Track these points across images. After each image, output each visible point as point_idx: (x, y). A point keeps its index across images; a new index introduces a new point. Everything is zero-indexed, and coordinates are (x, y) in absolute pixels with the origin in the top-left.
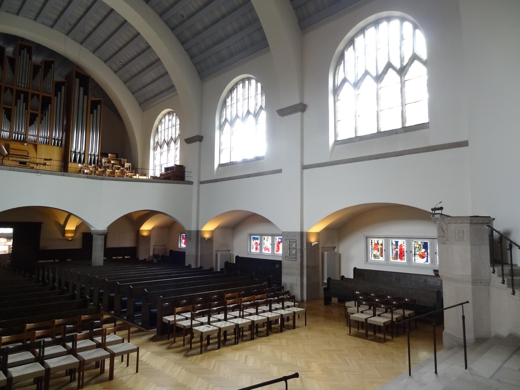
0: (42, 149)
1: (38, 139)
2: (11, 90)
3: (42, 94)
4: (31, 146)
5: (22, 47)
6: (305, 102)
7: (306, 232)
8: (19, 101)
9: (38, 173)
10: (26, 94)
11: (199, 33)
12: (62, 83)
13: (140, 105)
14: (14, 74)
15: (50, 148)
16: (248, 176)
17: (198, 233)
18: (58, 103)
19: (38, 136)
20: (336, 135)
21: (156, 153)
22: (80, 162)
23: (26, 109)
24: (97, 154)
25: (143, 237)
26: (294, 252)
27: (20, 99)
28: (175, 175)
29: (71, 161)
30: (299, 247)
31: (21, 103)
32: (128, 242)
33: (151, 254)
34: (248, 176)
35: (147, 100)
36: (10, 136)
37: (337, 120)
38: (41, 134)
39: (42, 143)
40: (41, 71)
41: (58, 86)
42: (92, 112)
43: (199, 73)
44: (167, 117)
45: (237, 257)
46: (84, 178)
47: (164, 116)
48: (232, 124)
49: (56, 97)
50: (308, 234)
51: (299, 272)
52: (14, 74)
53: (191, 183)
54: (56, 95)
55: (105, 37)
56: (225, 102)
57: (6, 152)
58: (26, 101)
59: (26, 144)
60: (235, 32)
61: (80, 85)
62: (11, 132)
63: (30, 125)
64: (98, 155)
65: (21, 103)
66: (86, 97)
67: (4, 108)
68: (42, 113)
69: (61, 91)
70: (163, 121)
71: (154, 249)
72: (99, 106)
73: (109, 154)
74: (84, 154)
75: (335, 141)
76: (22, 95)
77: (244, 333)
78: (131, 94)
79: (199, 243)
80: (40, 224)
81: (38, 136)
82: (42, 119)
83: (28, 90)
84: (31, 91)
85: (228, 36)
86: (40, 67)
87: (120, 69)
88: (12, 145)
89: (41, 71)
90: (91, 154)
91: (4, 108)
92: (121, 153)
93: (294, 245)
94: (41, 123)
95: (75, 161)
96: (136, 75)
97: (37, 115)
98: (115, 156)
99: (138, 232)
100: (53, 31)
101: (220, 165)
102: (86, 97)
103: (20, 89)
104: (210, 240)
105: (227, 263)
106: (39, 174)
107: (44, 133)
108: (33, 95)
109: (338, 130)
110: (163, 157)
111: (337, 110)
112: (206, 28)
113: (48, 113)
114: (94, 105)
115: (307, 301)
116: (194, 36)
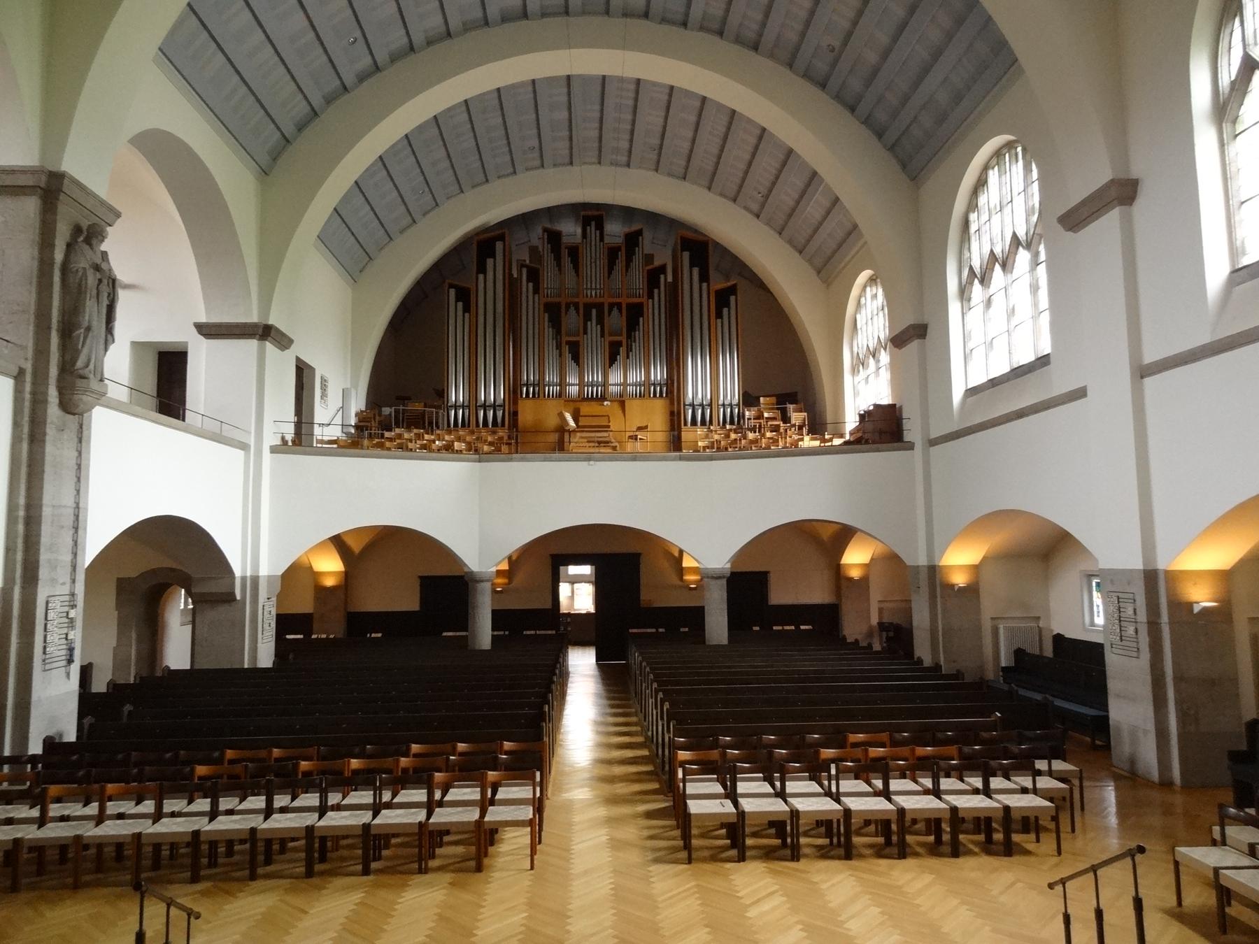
0: (633, 406)
1: (625, 389)
2: (576, 305)
3: (624, 301)
4: (616, 405)
6: (1135, 172)
7: (1166, 572)
9: (589, 460)
10: (600, 307)
11: (875, 71)
12: (662, 269)
13: (819, 272)
15: (646, 402)
16: (1020, 414)
17: (933, 570)
19: (625, 384)
20: (1235, 251)
21: (857, 379)
22: (703, 423)
23: (602, 335)
24: (735, 401)
25: (850, 579)
26: (1131, 630)
28: (884, 428)
29: (686, 424)
30: (1142, 616)
31: (593, 326)
32: (815, 593)
33: (874, 620)
34: (1020, 414)
35: (830, 258)
36: (581, 391)
37: (1234, 202)
39: (634, 396)
40: (622, 255)
41: (653, 276)
42: (719, 315)
43: (904, 166)
44: (868, 289)
45: (1059, 639)
46: (674, 460)
47: (865, 287)
48: (985, 280)
50: (1173, 577)
51: (1146, 691)
53: (911, 446)
54: (651, 296)
55: (715, 151)
56: (966, 224)
57: (572, 423)
58: (600, 321)
60: (949, 36)
61: (692, 265)
62: (581, 384)
64: (738, 405)
65: (593, 326)
66: (705, 285)
67: (568, 343)
68: (629, 337)
69: (659, 288)
70: (863, 300)
71: (881, 611)
72: (732, 298)
75: (1235, 271)
76: (594, 311)
77: (910, 839)
78: (797, 254)
79: (939, 599)
80: (638, 555)
81: (625, 384)
82: (629, 349)
83: (602, 300)
84: (607, 300)
85: (937, 54)
86: (619, 249)
87: (763, 205)
88: (586, 409)
89: (622, 255)
90: (724, 405)
91: (568, 343)
92: (788, 387)
93: (1130, 611)
95: (694, 422)
96: (794, 210)
97: (619, 344)
98: (774, 400)
99: (837, 570)
100: (633, 172)
101: (971, 392)
102: (705, 285)
103: (588, 300)
104: (972, 591)
105: (1019, 654)
107: (636, 376)
108: (611, 306)
109: (1240, 234)
110: (864, 389)
111: (1232, 169)
112: (885, 54)
113: (639, 335)
114: (723, 299)
115: (1187, 786)
116: (869, 81)
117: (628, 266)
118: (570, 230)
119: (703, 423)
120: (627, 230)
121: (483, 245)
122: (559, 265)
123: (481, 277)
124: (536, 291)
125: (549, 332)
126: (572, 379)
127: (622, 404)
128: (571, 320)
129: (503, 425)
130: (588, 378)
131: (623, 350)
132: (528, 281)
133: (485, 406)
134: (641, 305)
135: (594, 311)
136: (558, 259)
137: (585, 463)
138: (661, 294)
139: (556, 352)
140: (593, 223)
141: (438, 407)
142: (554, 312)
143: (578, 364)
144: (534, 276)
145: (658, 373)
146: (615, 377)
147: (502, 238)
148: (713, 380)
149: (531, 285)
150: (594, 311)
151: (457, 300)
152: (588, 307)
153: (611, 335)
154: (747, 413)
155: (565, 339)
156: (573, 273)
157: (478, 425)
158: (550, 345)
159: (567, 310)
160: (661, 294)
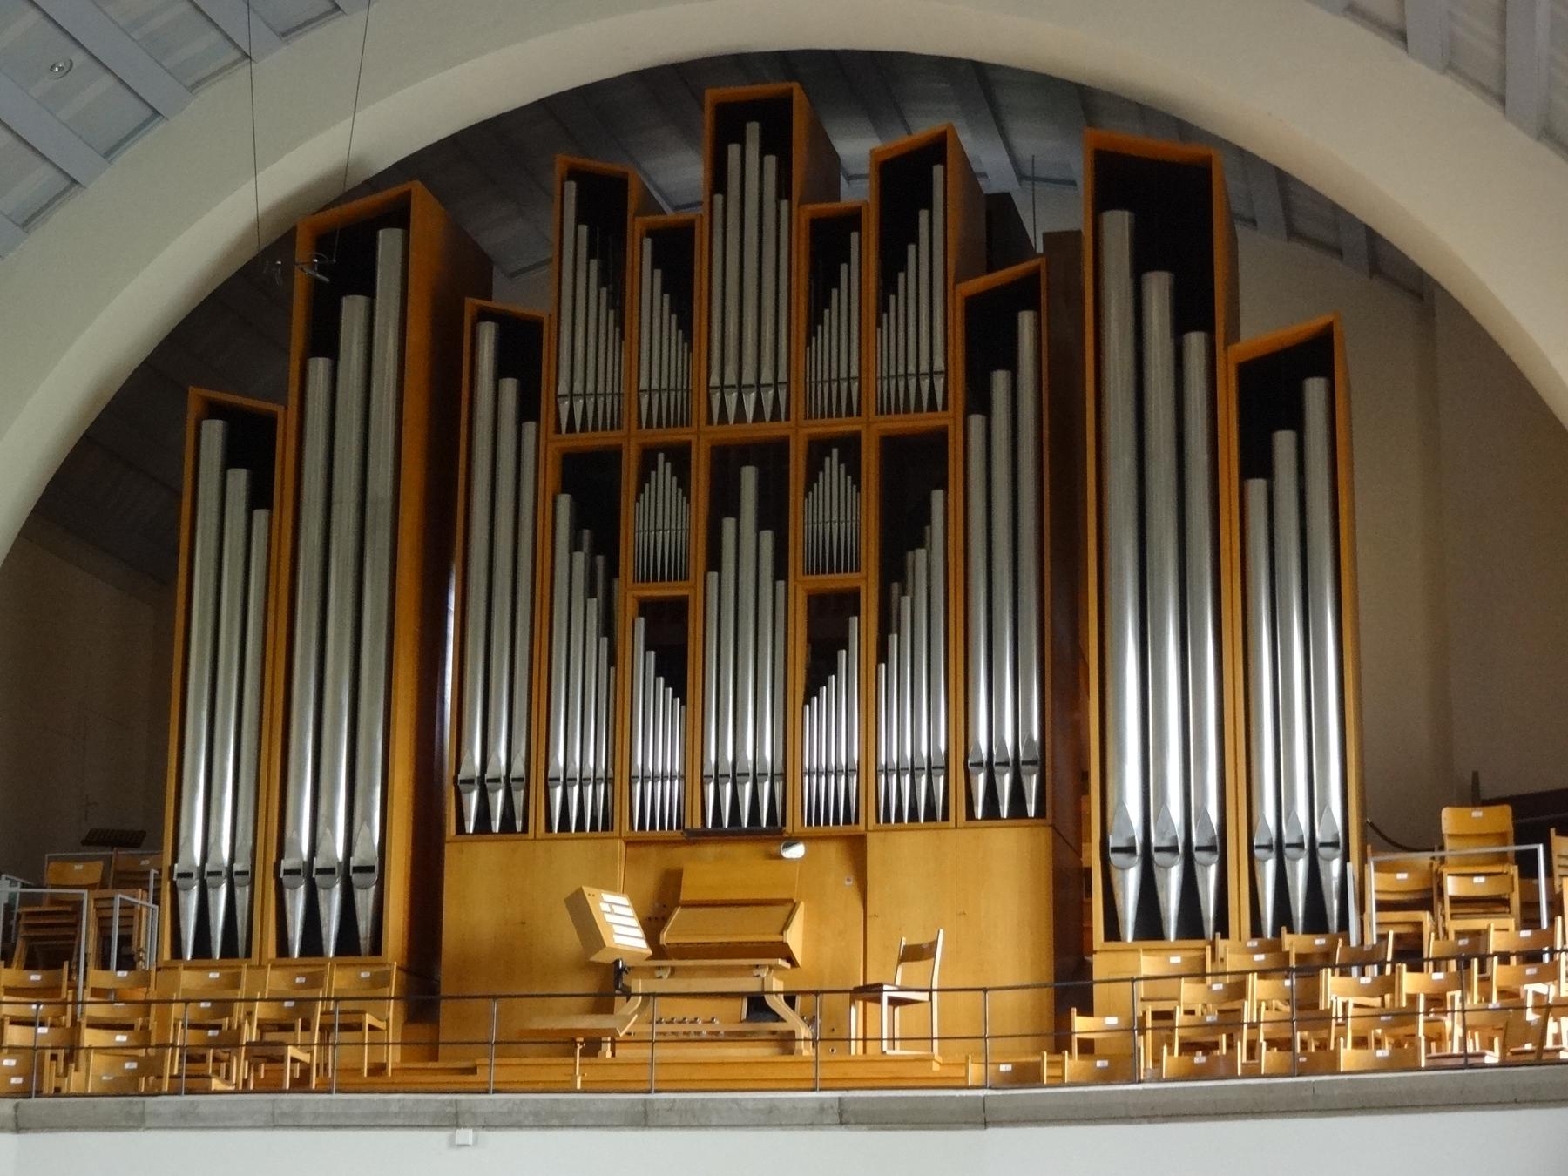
0: (901, 856)
3: (871, 429)
4: (832, 854)
5: (728, 125)
8: (729, 524)
9: (454, 1121)
10: (771, 456)
14: (688, 338)
18: (995, 468)
19: (870, 767)
23: (780, 572)
27: (736, 513)
31: (745, 535)
38: (889, 752)
40: (864, 247)
42: (1257, 462)
46: (815, 1120)
49: (976, 421)
52: (688, 338)
54: (979, 401)
58: (773, 515)
59: (797, 851)
61: (1141, 266)
62: (693, 771)
63: (811, 692)
65: (745, 535)
66: (1195, 342)
69: (1012, 365)
72: (1314, 389)
73: (1449, 819)
74: (1219, 847)
76: (749, 475)
84: (799, 433)
86: (853, 219)
89: (864, 247)
90: (1279, 848)
91: (648, 608)
94: (883, 656)
95: (1150, 926)
97: (848, 602)
98: (1501, 818)
103: (732, 432)
106: (465, 1135)
107: (913, 732)
108: (818, 449)
114: (1273, 393)
117: (888, 285)
118: (676, 173)
119: (1191, 925)
120: (900, 140)
121: (326, 251)
122: (617, 302)
123: (320, 366)
124: (528, 408)
125: (571, 566)
126: (657, 751)
127: (856, 848)
128: (658, 516)
129: (376, 947)
130: (719, 750)
131: (863, 629)
132: (501, 372)
133: (311, 876)
134: (936, 441)
135: (754, 473)
136: (613, 278)
137: (440, 1137)
138: (1019, 390)
139: (597, 646)
140: (753, 130)
141: (134, 879)
142: (591, 491)
143: (680, 692)
144: (523, 349)
145: (1007, 717)
146: (830, 735)
147: (398, 215)
148: (1234, 733)
149: (510, 386)
150: (754, 473)
151: (231, 459)
152: (726, 461)
153: (810, 570)
154: (1374, 881)
155: (629, 594)
156: (677, 336)
157: (283, 948)
158: (577, 616)
159: (644, 478)
160: (1019, 390)
